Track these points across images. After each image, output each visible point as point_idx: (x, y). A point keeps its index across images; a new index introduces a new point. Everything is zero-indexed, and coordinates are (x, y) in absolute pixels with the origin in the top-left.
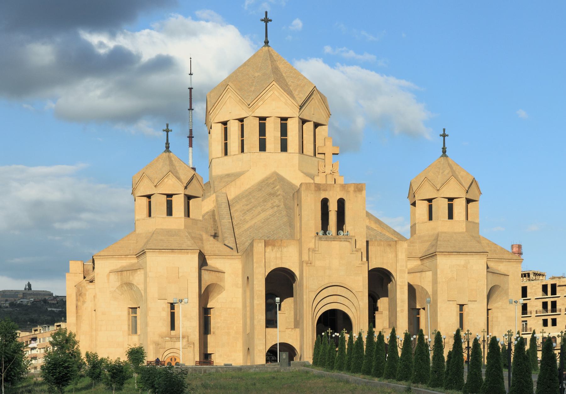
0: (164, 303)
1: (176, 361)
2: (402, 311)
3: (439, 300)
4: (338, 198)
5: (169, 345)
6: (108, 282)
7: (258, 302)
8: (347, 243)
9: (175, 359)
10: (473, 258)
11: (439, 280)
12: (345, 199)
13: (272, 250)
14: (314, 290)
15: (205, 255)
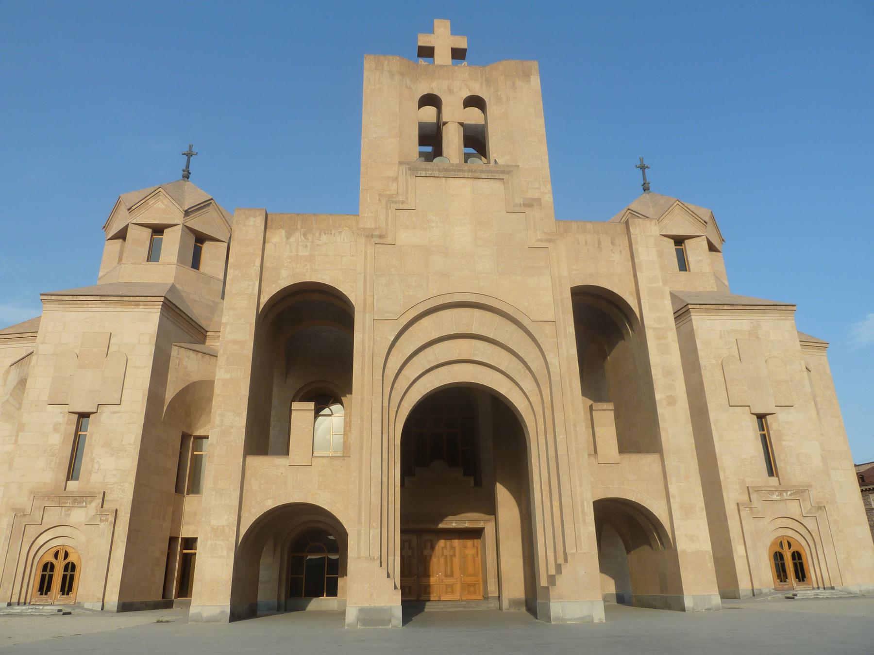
0: (61, 413)
1: (69, 560)
2: (672, 401)
3: (710, 406)
4: (466, 94)
5: (53, 516)
6: (4, 385)
7: (228, 376)
8: (496, 185)
9: (66, 555)
10: (765, 318)
11: (703, 362)
12: (484, 97)
13: (288, 238)
14: (392, 316)
15: (207, 330)
